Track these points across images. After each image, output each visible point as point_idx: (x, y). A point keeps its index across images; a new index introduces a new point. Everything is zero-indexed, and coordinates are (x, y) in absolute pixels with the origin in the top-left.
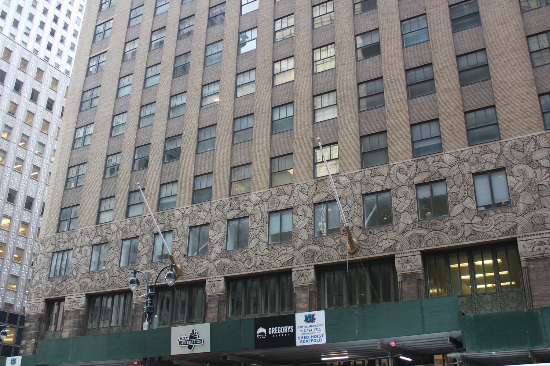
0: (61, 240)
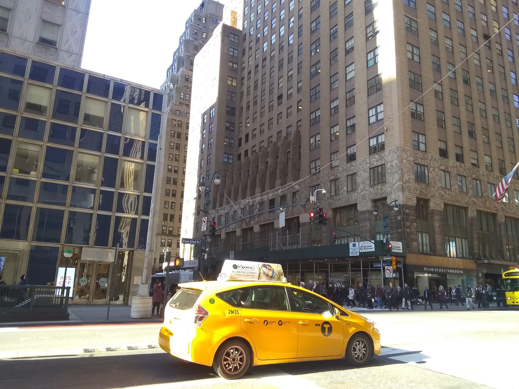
0: (418, 155)
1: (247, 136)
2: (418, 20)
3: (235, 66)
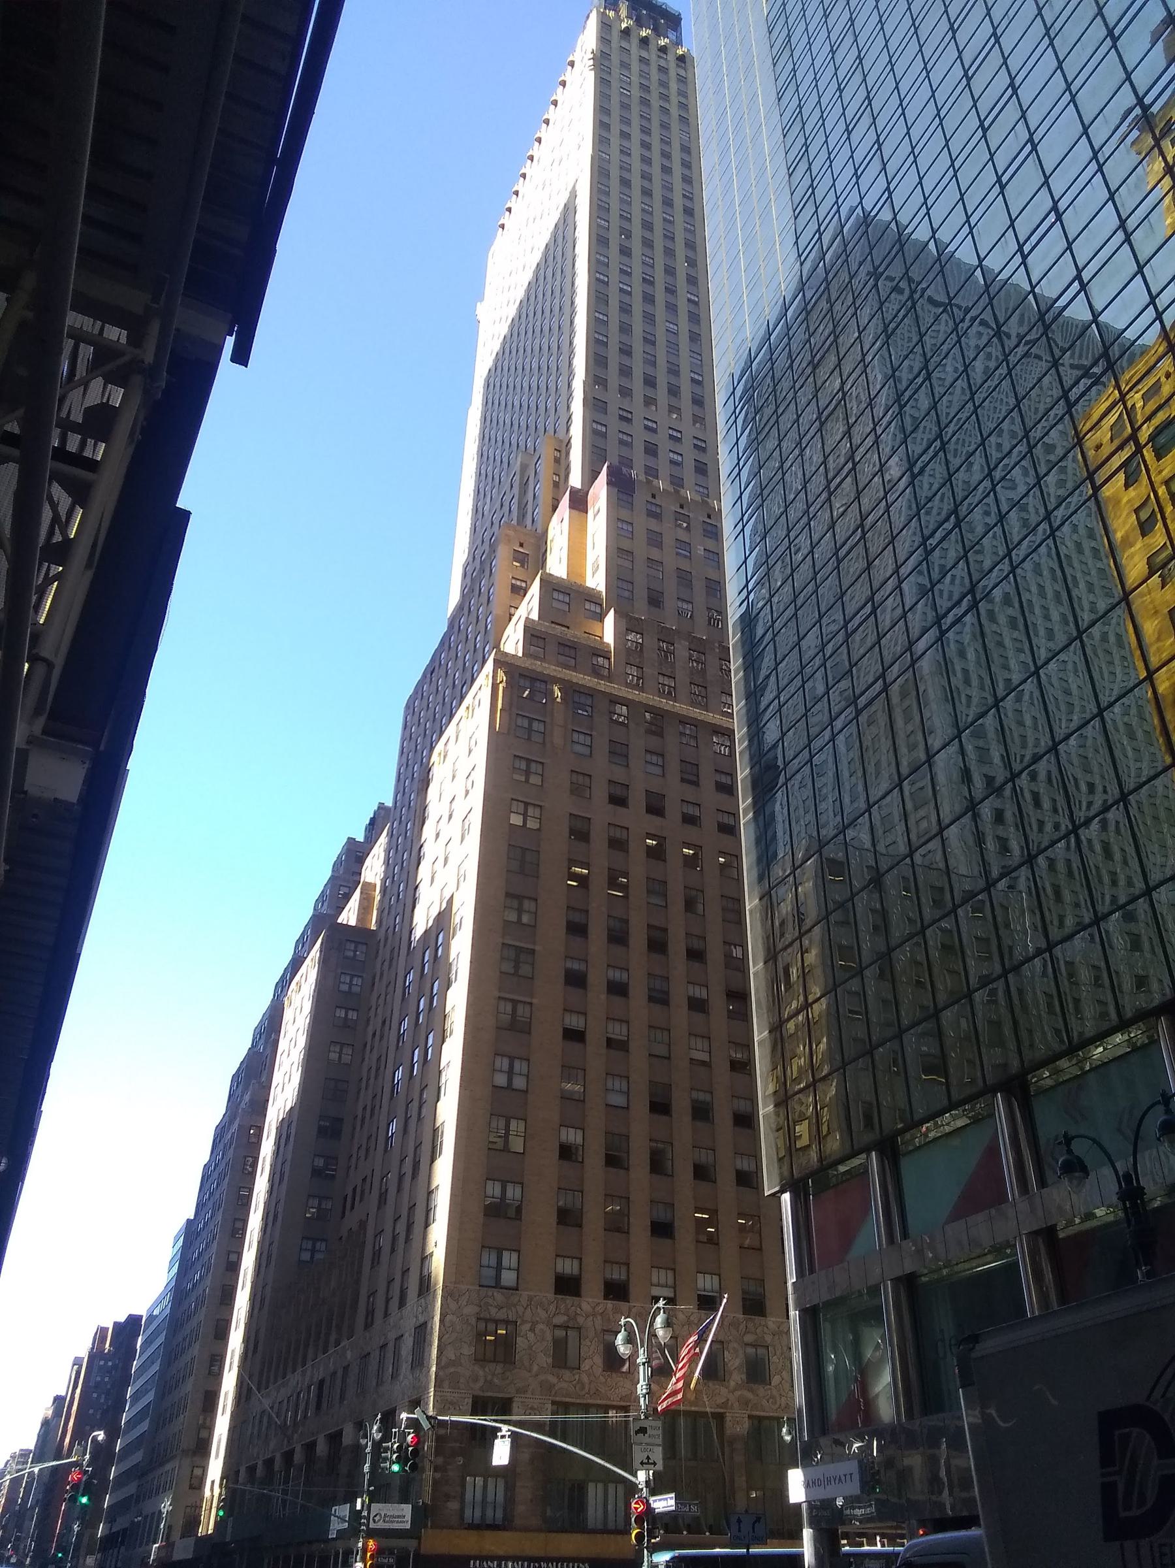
0: (490, 1301)
1: (354, 1190)
2: (535, 1001)
3: (352, 1015)
